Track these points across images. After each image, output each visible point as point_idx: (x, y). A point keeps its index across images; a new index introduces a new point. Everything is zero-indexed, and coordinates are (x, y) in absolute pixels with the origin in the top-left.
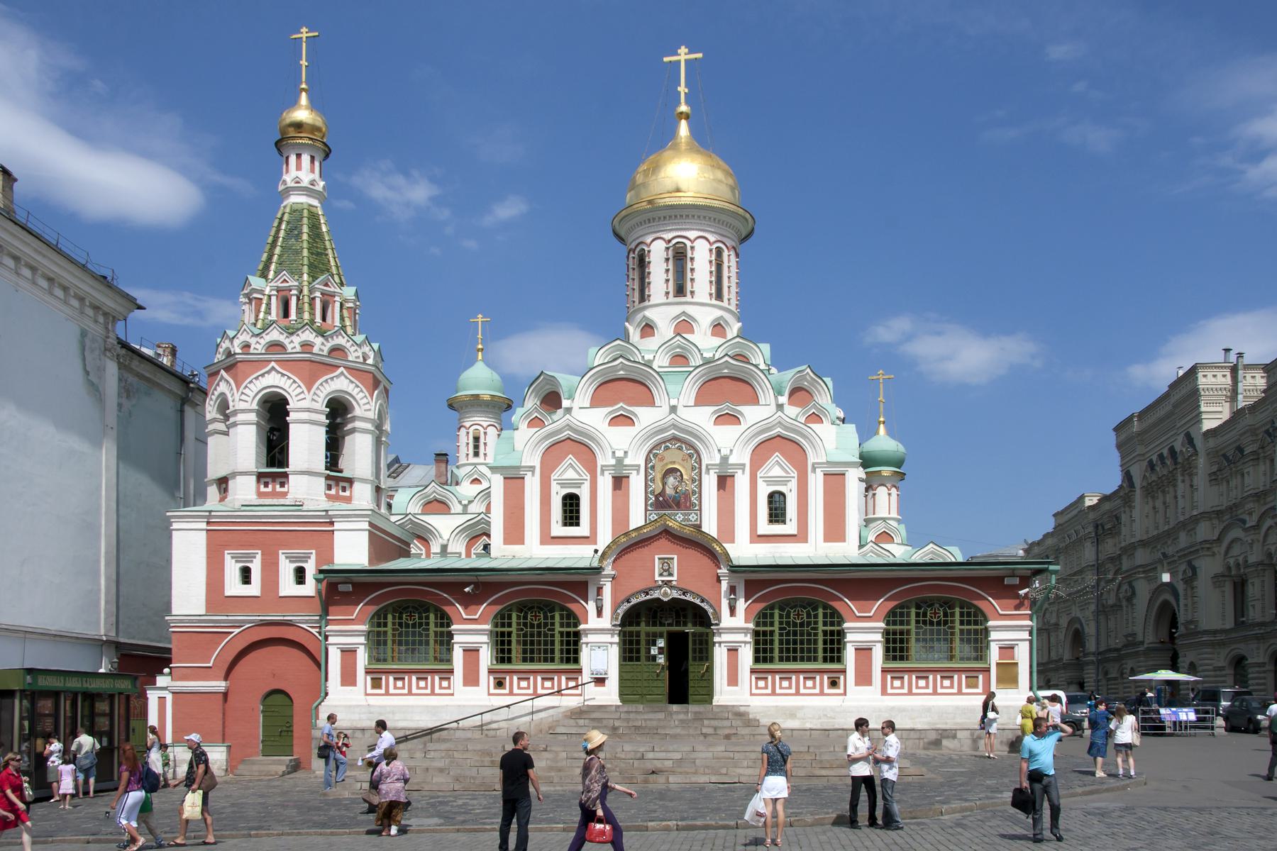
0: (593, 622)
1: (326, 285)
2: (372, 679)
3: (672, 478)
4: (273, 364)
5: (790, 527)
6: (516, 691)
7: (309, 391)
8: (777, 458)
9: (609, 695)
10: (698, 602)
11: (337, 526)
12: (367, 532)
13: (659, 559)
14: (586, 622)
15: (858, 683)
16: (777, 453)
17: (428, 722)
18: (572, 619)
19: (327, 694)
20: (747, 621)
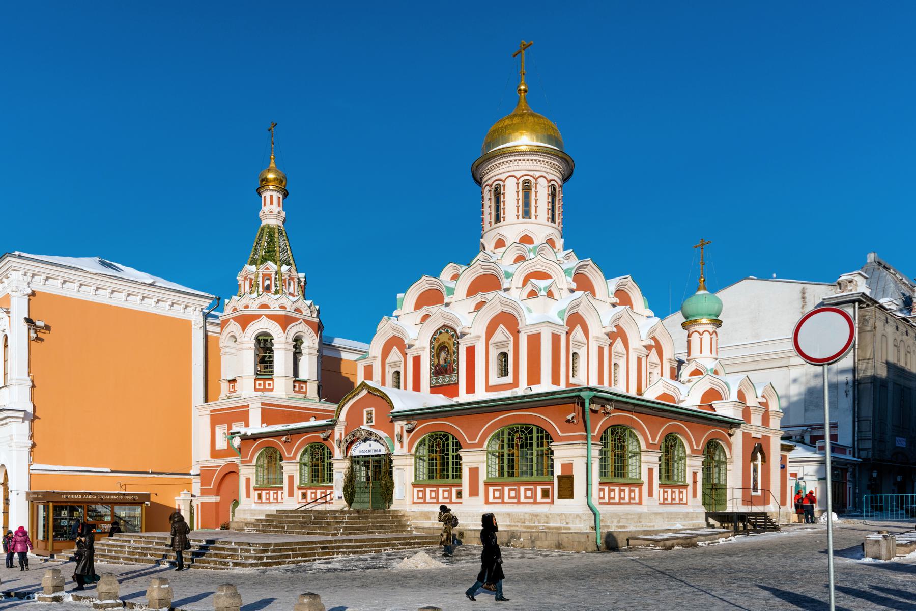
3: (443, 353)
5: (509, 379)
7: (243, 331)
13: (367, 411)
18: (331, 455)
20: (409, 450)
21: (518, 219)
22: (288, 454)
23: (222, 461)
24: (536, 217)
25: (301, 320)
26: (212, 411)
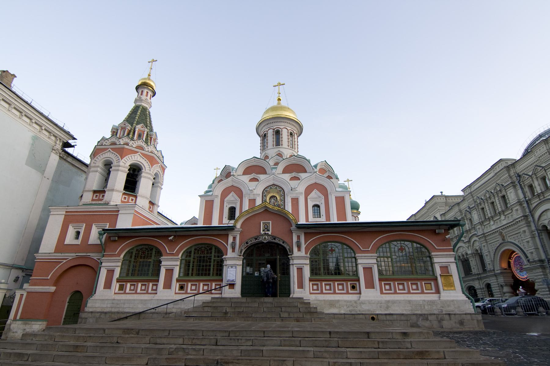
0: (230, 254)
1: (142, 127)
2: (120, 285)
4: (110, 149)
6: (189, 291)
8: (315, 191)
9: (236, 292)
10: (281, 243)
11: (120, 212)
12: (133, 215)
13: (263, 223)
14: (227, 255)
15: (366, 288)
16: (315, 189)
17: (140, 308)
18: (220, 253)
19: (95, 293)
20: (306, 253)
22: (169, 251)
23: (74, 254)
24: (295, 148)
25: (160, 164)
26: (66, 211)
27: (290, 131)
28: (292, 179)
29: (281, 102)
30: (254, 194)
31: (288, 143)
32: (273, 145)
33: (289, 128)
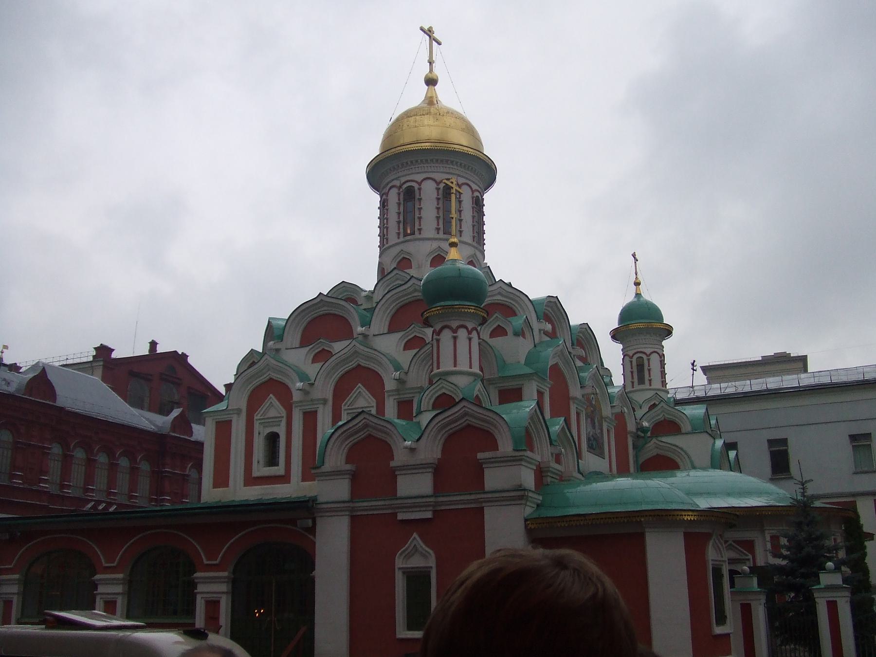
21: (438, 233)
27: (442, 186)
28: (408, 346)
29: (439, 89)
30: (312, 400)
31: (438, 222)
32: (399, 234)
33: (438, 177)
